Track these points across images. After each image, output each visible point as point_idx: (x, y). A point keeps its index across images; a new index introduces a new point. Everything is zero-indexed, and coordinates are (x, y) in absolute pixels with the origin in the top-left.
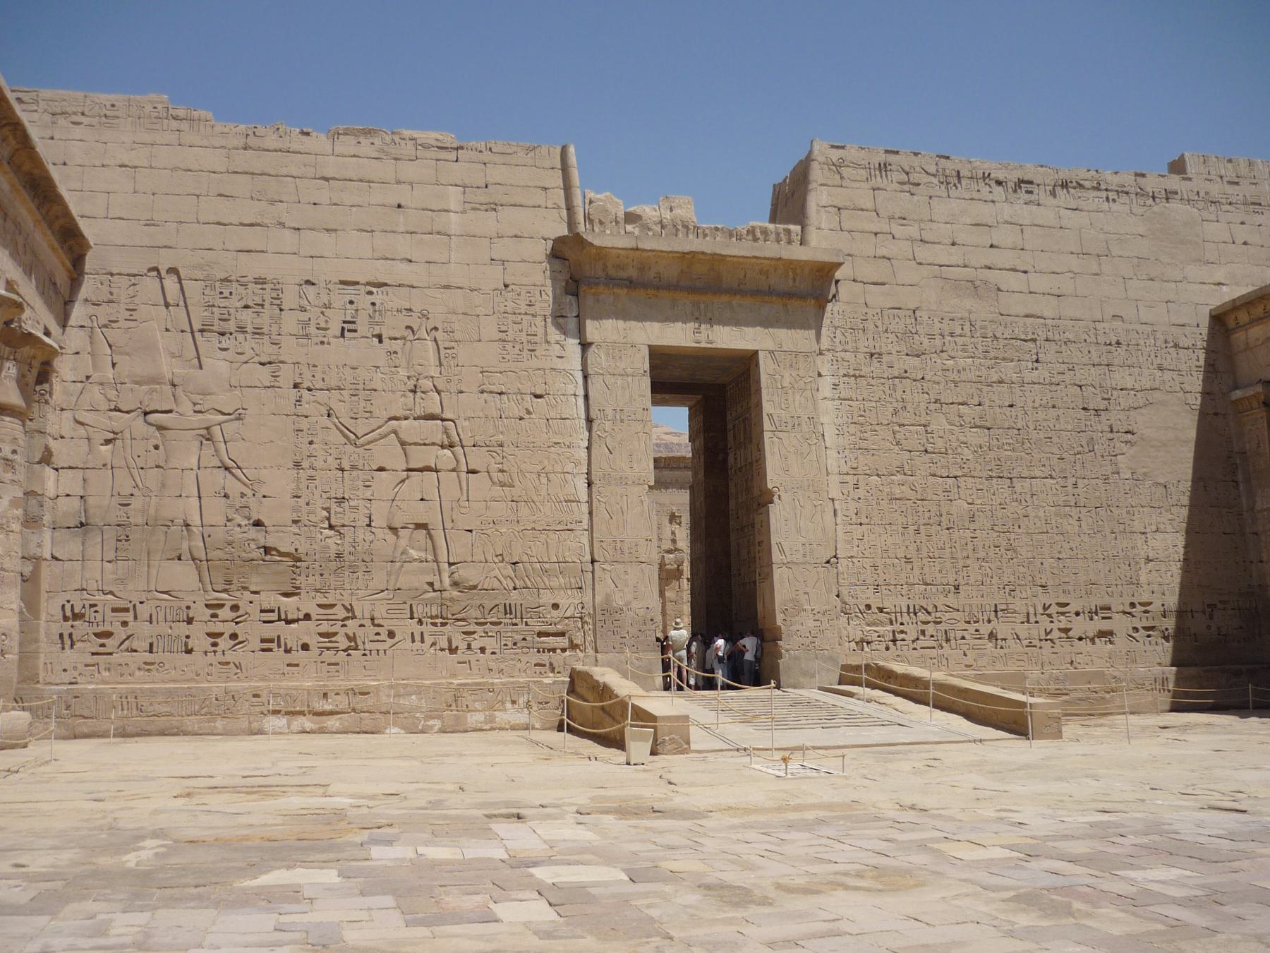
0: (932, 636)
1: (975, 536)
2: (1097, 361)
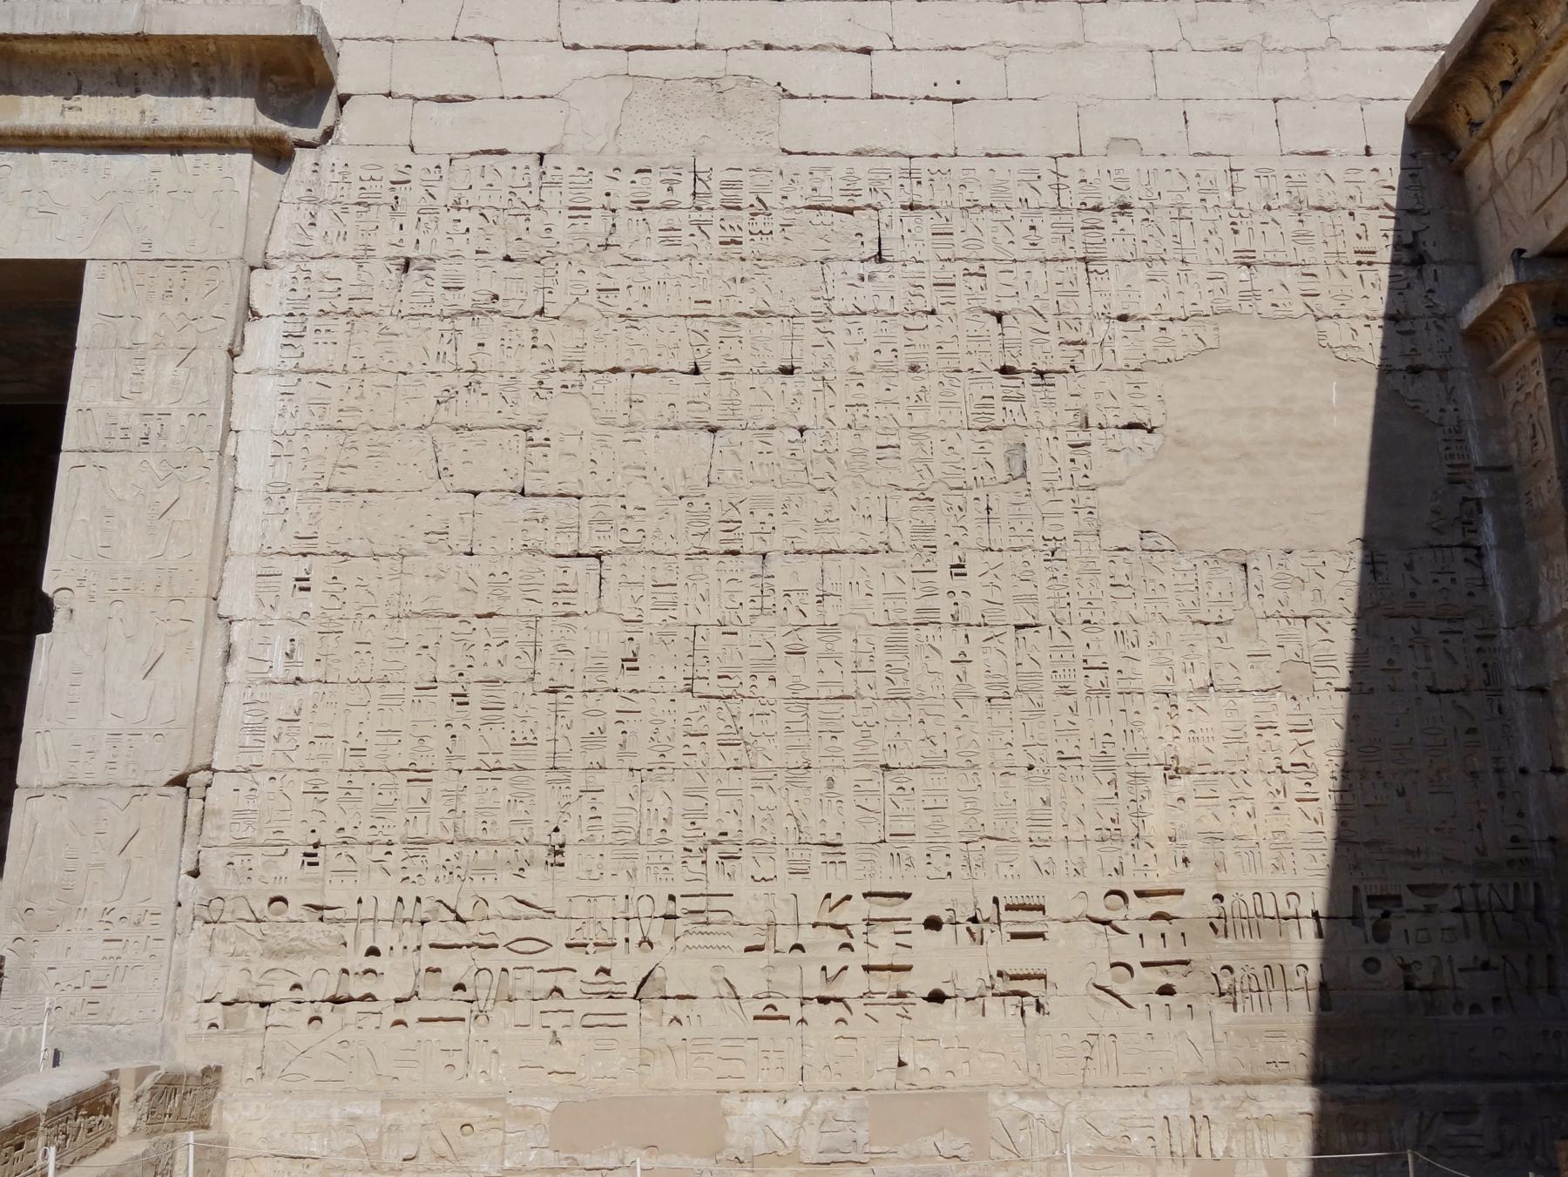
0: (460, 987)
1: (634, 707)
2: (1051, 248)
